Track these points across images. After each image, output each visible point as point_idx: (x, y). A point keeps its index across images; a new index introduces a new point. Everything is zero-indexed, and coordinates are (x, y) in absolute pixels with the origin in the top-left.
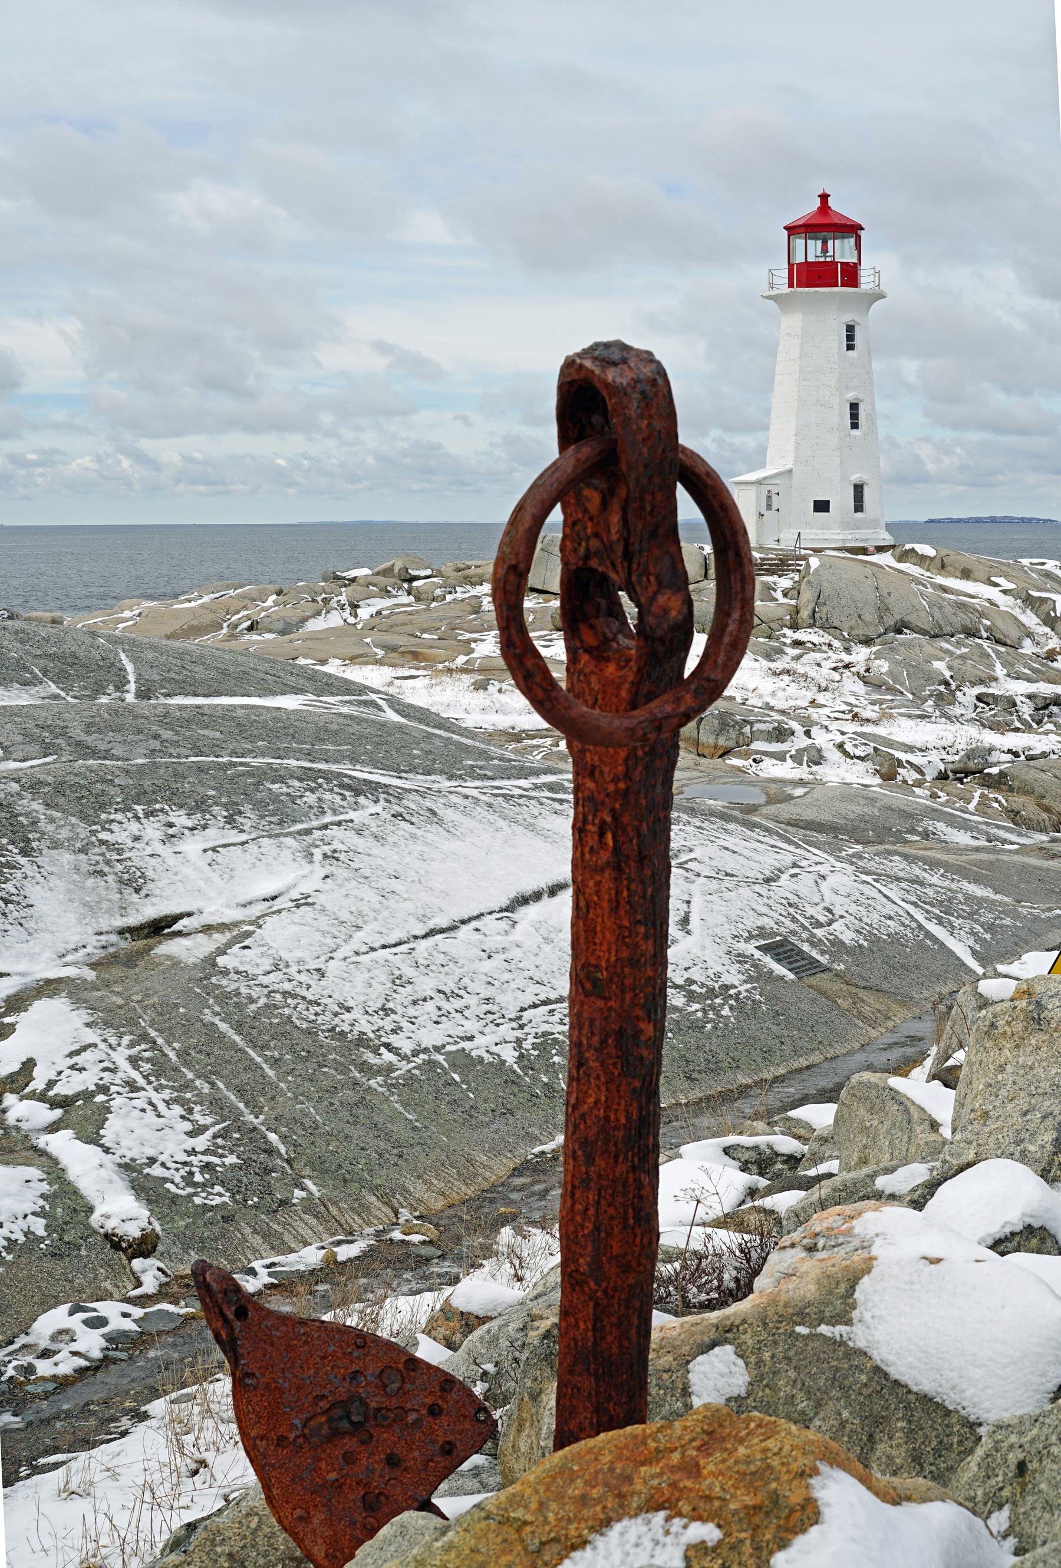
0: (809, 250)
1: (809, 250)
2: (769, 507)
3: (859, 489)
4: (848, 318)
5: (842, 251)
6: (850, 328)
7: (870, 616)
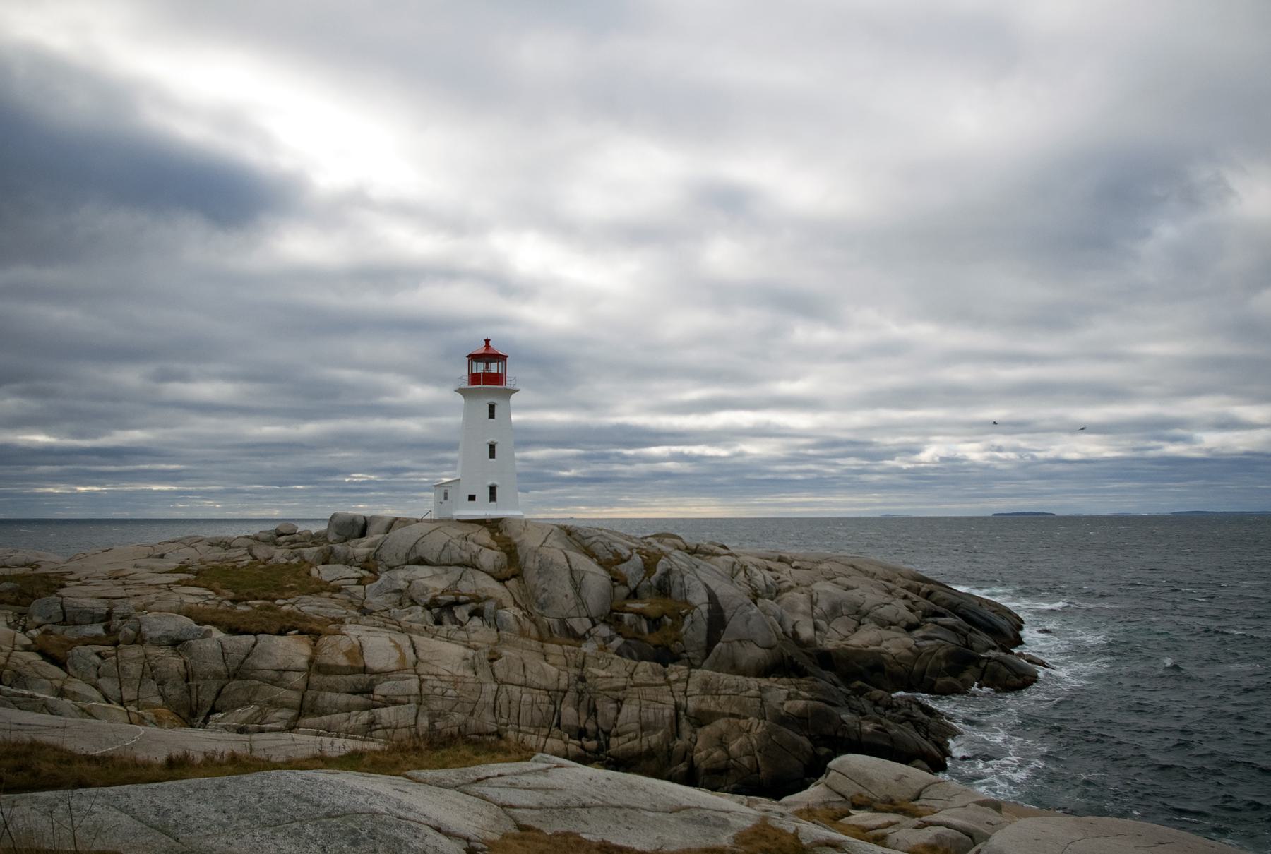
0: (479, 368)
1: (479, 368)
2: (446, 498)
3: (493, 490)
4: (490, 400)
5: (494, 368)
6: (492, 408)
7: (401, 555)
